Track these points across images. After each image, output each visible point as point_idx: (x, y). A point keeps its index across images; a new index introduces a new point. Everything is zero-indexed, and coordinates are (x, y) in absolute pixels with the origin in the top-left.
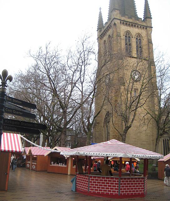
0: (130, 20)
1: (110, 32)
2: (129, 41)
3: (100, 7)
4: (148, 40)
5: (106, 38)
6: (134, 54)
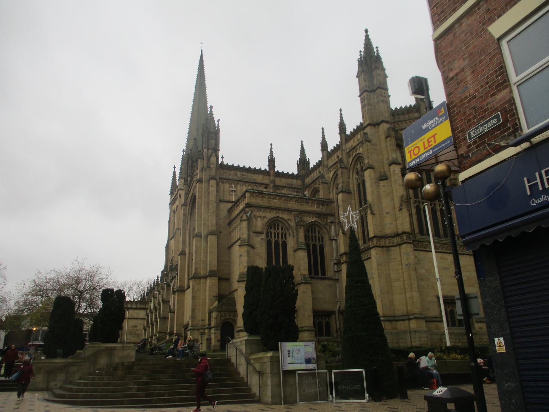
3: (175, 166)
5: (175, 206)
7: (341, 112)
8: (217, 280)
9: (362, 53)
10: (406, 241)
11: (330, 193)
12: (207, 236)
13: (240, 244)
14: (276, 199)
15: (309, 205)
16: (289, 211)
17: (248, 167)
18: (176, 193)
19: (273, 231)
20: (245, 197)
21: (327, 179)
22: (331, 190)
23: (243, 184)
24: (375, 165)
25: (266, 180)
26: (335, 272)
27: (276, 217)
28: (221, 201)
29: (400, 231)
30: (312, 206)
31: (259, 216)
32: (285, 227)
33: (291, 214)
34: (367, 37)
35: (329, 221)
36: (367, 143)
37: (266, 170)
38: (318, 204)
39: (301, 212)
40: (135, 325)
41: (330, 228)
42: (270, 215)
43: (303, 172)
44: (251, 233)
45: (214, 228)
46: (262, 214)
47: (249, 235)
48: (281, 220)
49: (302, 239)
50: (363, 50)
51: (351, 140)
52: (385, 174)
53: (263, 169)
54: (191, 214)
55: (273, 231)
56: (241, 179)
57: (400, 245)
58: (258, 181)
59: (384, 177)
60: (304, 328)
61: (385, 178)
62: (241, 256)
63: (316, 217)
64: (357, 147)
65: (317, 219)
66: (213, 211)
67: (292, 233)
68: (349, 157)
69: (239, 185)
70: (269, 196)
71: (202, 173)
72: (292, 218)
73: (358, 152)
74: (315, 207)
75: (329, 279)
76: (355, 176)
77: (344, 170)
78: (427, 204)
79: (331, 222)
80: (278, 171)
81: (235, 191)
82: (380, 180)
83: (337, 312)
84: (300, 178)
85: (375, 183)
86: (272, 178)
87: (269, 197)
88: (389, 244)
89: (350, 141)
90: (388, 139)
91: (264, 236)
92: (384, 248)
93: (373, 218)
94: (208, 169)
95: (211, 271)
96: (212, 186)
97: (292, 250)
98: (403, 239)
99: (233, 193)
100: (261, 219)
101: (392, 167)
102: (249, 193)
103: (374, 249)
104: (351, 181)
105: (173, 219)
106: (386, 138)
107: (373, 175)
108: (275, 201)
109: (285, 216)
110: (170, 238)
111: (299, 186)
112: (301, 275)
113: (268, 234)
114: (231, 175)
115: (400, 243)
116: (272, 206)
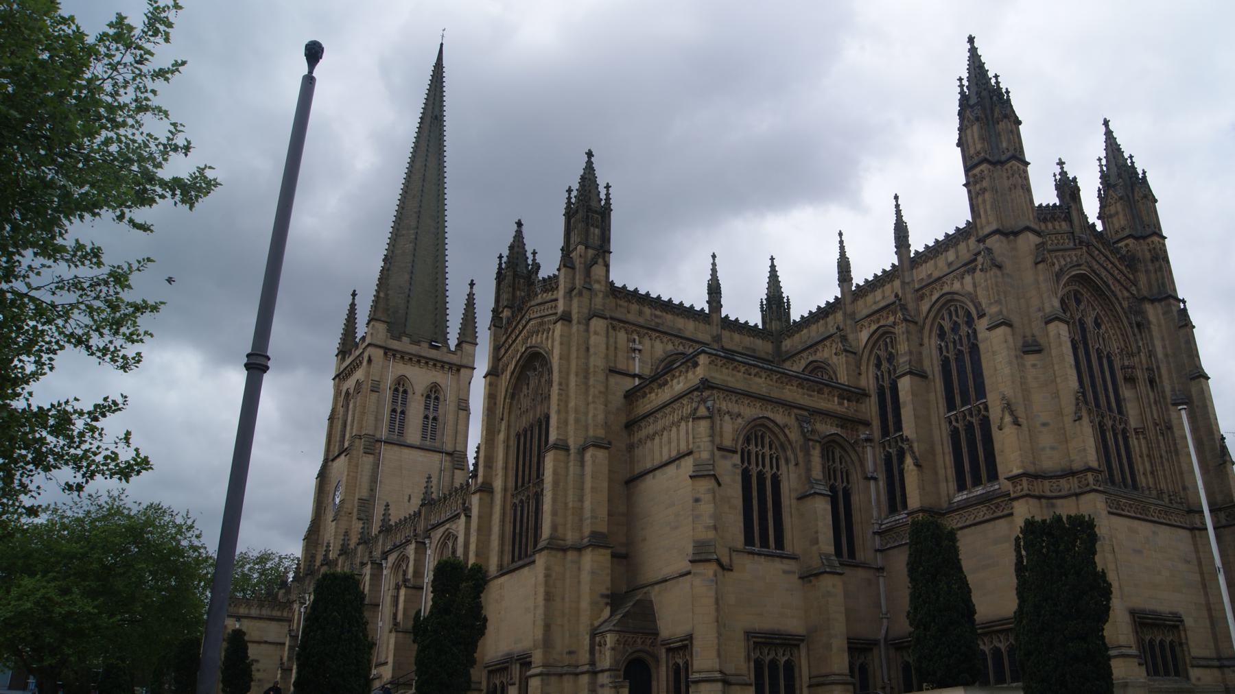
0: (413, 349)
1: (359, 374)
2: (404, 403)
3: (355, 291)
5: (350, 383)
6: (413, 433)
7: (897, 201)
8: (609, 557)
9: (965, 83)
10: (1094, 487)
11: (860, 374)
12: (582, 450)
13: (694, 474)
14: (761, 377)
15: (823, 396)
16: (788, 406)
17: (666, 300)
18: (358, 353)
19: (752, 448)
20: (696, 365)
21: (854, 344)
22: (863, 368)
23: (668, 341)
24: (1015, 319)
25: (703, 333)
26: (877, 551)
27: (760, 418)
28: (613, 371)
29: (1077, 466)
30: (829, 400)
31: (728, 412)
32: (777, 443)
33: (789, 414)
34: (973, 52)
35: (862, 436)
36: (995, 270)
37: (702, 310)
38: (841, 397)
39: (813, 411)
41: (863, 453)
42: (751, 411)
43: (775, 326)
44: (716, 452)
45: (601, 433)
46: (735, 409)
47: (713, 454)
48: (771, 425)
49: (817, 472)
50: (965, 75)
51: (926, 262)
52: (1035, 341)
53: (698, 308)
54: (513, 396)
55: (752, 448)
56: (653, 325)
57: (1077, 495)
58: (687, 334)
59: (1032, 348)
60: (833, 678)
61: (1037, 348)
62: (697, 500)
63: (837, 426)
64: (944, 279)
65: (839, 431)
66: (600, 392)
67: (792, 457)
68: (922, 298)
69: (647, 338)
70: (747, 367)
71: (571, 300)
72: (792, 421)
73: (946, 289)
74: (834, 402)
75: (864, 566)
76: (935, 341)
77: (912, 327)
78: (1185, 407)
79: (867, 440)
80: (727, 317)
81: (640, 351)
82: (1026, 353)
83: (882, 641)
84: (771, 337)
85: (1016, 357)
86: (715, 330)
87: (747, 370)
88: (1051, 491)
89: (924, 265)
90: (1041, 266)
91: (737, 459)
92: (1044, 501)
93: (1018, 434)
94: (585, 291)
95: (594, 534)
96: (596, 333)
97: (794, 495)
98: (1084, 482)
99: (637, 355)
100: (732, 419)
101: (1052, 327)
102: (707, 356)
103: (1021, 501)
104: (925, 352)
105: (341, 413)
106: (1037, 264)
107: (1010, 339)
108: (757, 380)
109: (780, 417)
110: (331, 458)
111: (767, 353)
112: (820, 554)
113: (745, 456)
114: (632, 313)
115: (1078, 491)
116: (754, 391)
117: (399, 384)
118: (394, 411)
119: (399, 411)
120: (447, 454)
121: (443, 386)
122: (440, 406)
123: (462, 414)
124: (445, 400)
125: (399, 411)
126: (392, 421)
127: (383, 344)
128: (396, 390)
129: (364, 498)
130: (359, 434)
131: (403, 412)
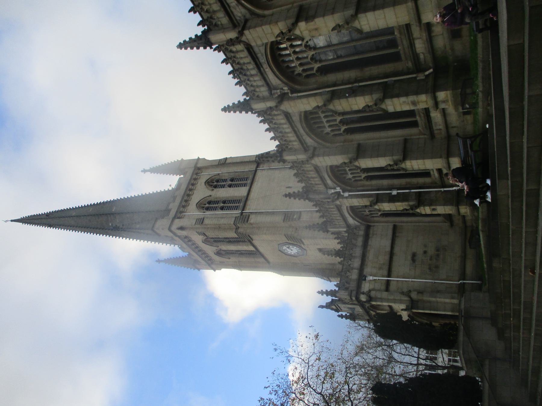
2: (217, 202)
4: (221, 164)
40: (409, 258)
117: (203, 207)
118: (222, 208)
119: (222, 205)
120: (257, 167)
121: (208, 177)
122: (223, 178)
123: (228, 161)
124: (219, 174)
125: (222, 205)
126: (229, 208)
127: (171, 220)
128: (207, 209)
129: (283, 218)
130: (234, 230)
131: (224, 202)
